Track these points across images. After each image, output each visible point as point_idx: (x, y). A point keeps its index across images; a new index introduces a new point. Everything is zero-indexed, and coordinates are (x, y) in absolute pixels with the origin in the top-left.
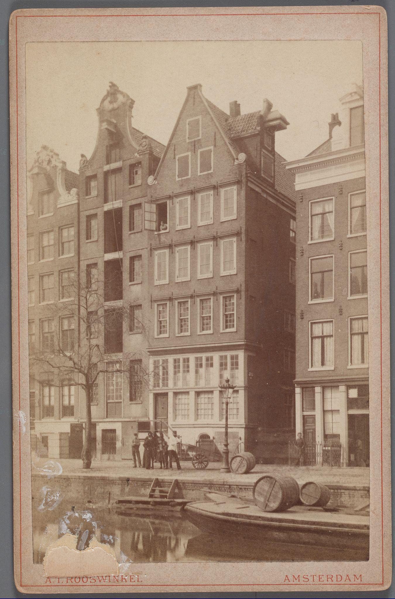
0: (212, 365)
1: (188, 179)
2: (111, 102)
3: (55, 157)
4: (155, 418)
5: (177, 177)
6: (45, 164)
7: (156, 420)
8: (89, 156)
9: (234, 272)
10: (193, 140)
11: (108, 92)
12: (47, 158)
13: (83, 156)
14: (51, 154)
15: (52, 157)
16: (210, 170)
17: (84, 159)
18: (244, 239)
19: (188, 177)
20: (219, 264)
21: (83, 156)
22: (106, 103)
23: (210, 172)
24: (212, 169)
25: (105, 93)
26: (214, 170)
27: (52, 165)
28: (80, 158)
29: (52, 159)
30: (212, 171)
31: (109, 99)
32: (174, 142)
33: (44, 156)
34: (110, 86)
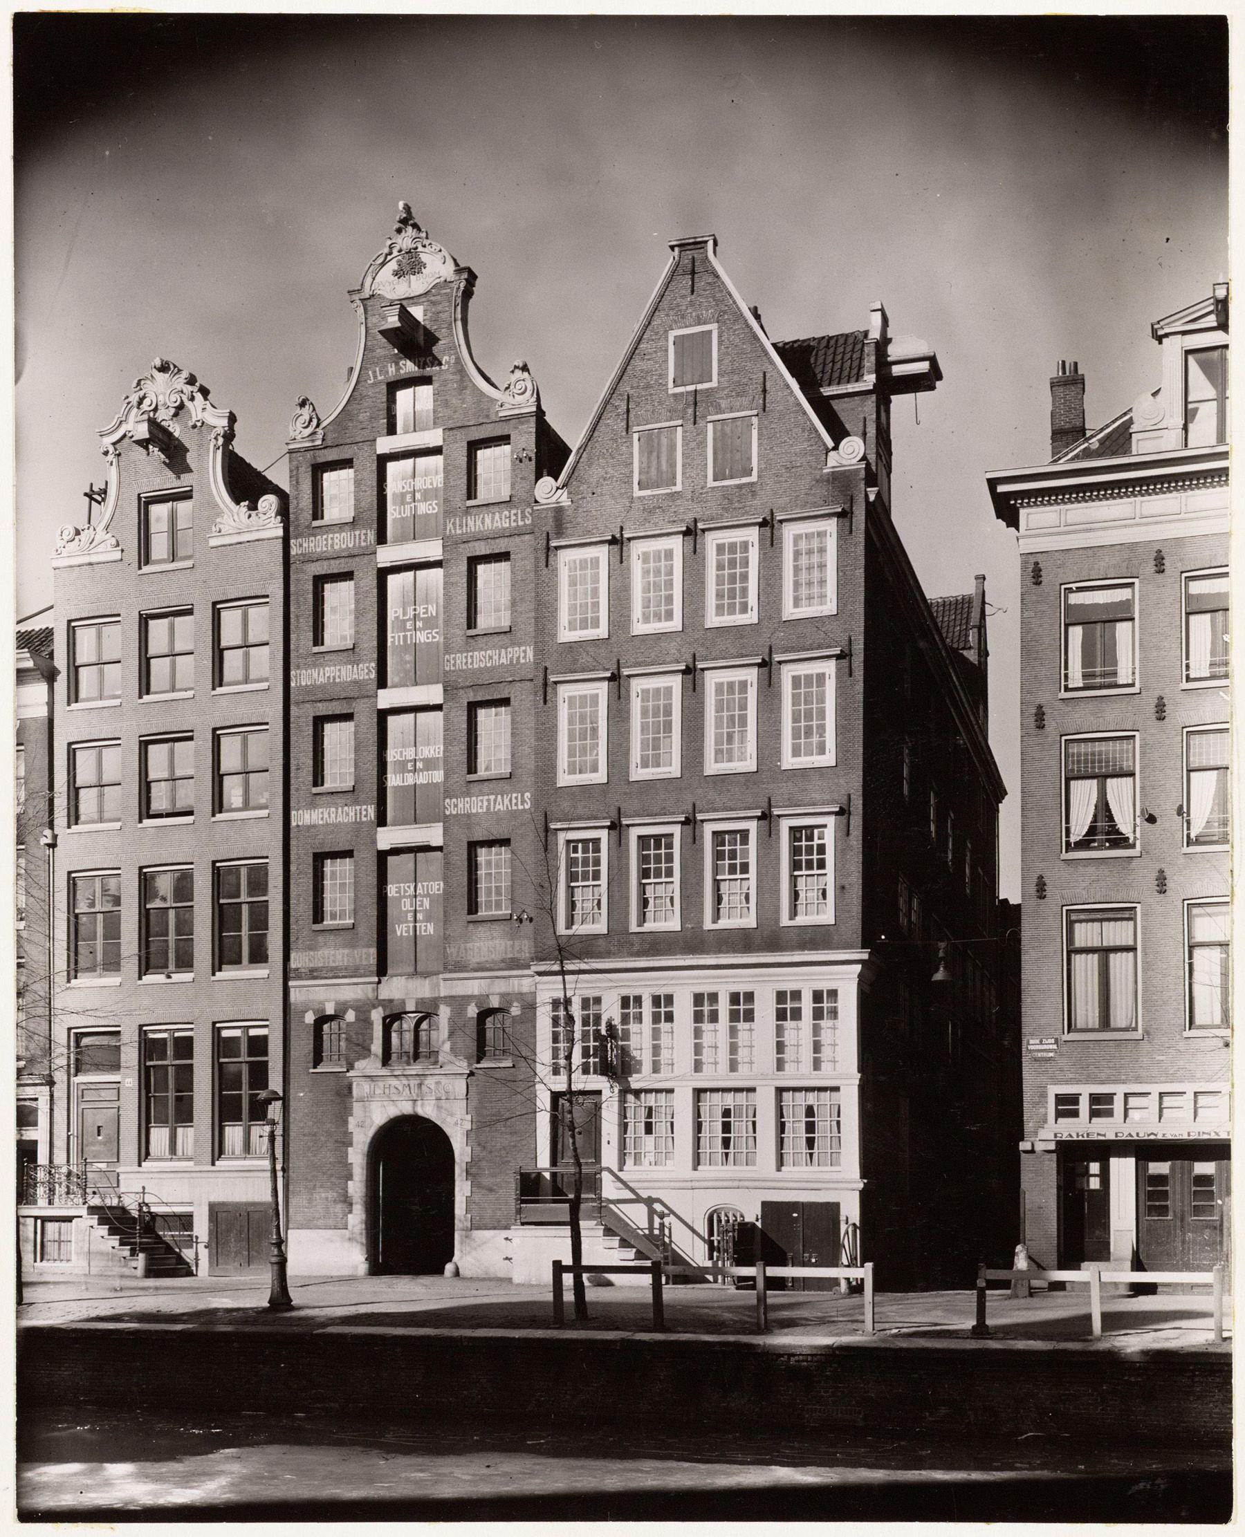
0: (749, 1016)
1: (673, 496)
3: (199, 396)
4: (554, 1162)
5: (636, 486)
6: (163, 416)
7: (555, 1170)
9: (829, 759)
10: (691, 388)
12: (173, 400)
14: (188, 389)
15: (192, 399)
16: (748, 472)
17: (306, 412)
19: (674, 489)
20: (778, 735)
23: (745, 480)
24: (755, 473)
26: (759, 477)
27: (191, 424)
29: (188, 404)
30: (754, 478)
32: (625, 388)
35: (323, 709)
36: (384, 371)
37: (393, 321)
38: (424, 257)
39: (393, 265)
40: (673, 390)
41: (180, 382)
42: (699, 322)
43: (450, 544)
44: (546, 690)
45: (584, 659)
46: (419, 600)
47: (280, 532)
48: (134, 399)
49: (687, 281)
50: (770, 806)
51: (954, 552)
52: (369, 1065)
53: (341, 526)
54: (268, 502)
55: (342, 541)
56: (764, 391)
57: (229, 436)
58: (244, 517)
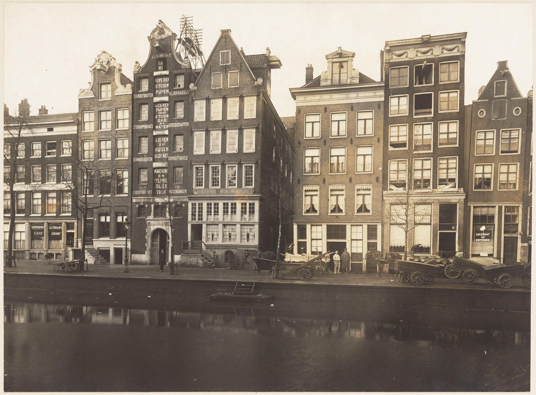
1: (220, 89)
2: (160, 34)
3: (113, 59)
6: (105, 64)
8: (143, 63)
11: (158, 27)
12: (107, 60)
13: (137, 62)
14: (110, 58)
17: (137, 64)
18: (260, 131)
21: (137, 62)
22: (156, 33)
25: (156, 27)
28: (135, 64)
31: (157, 32)
32: (210, 63)
33: (104, 58)
34: (159, 23)
35: (141, 135)
36: (155, 56)
37: (157, 45)
38: (165, 30)
39: (157, 32)
40: (221, 65)
41: (108, 56)
42: (227, 49)
43: (170, 98)
44: (192, 133)
45: (200, 125)
46: (163, 111)
47: (131, 93)
48: (97, 59)
49: (224, 40)
50: (241, 161)
51: (285, 108)
52: (151, 217)
53: (146, 92)
54: (129, 86)
55: (146, 96)
56: (241, 66)
57: (120, 70)
58: (123, 89)
